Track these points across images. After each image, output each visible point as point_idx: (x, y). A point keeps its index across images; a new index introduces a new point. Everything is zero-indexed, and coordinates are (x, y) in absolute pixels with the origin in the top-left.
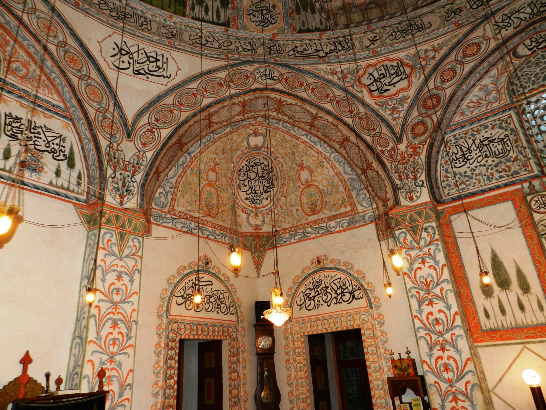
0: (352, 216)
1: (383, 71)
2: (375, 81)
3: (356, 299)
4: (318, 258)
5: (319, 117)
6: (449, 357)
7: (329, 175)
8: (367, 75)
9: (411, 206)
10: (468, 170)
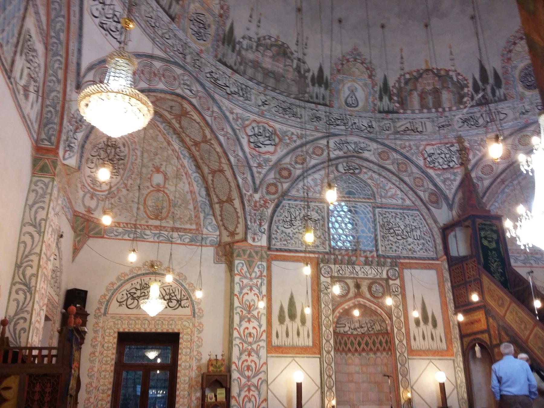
0: (195, 235)
1: (261, 131)
2: (255, 135)
3: (182, 307)
4: (152, 261)
5: (211, 143)
6: (252, 361)
7: (183, 190)
8: (250, 127)
9: (252, 245)
10: (291, 233)
